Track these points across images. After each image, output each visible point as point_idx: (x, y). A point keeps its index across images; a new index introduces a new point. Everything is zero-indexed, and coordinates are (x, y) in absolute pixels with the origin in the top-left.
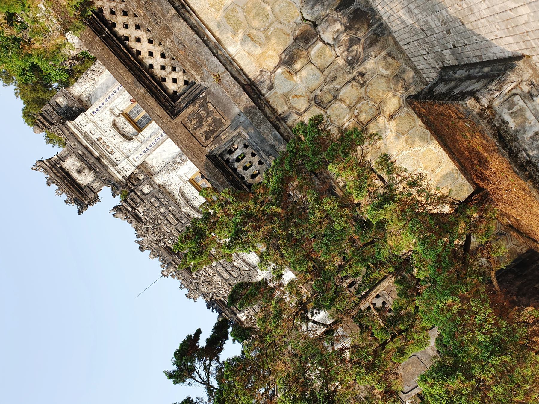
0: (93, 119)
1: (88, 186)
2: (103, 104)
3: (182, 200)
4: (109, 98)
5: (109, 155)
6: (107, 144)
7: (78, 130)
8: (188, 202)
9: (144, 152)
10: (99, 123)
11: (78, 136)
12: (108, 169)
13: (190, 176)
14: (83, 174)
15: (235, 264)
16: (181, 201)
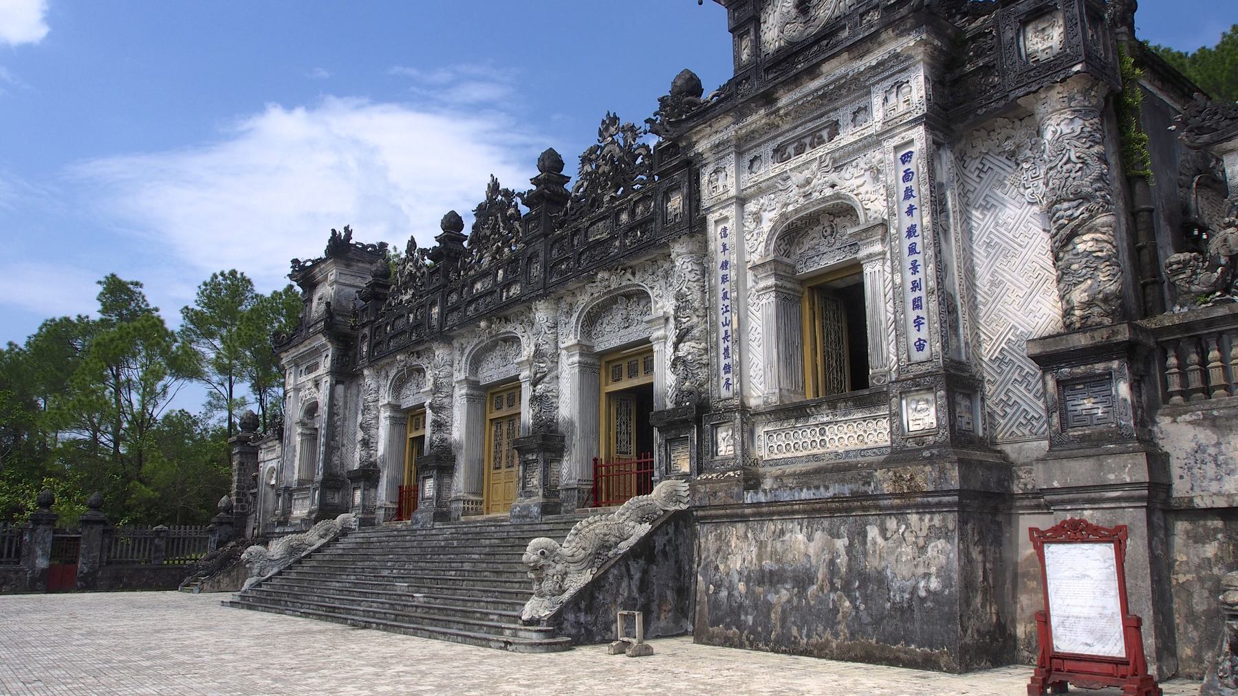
0: (890, 144)
1: (756, 21)
2: (910, 211)
3: (626, 286)
4: (912, 250)
5: (780, 140)
6: (808, 150)
7: (879, 64)
8: (628, 296)
9: (725, 265)
10: (875, 156)
11: (861, 57)
12: (729, 119)
13: (656, 348)
14: (794, 12)
15: (483, 324)
16: (623, 284)
